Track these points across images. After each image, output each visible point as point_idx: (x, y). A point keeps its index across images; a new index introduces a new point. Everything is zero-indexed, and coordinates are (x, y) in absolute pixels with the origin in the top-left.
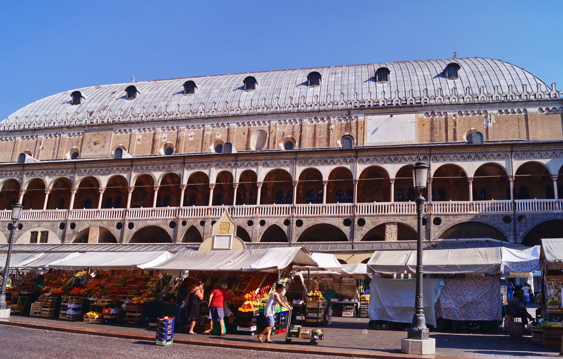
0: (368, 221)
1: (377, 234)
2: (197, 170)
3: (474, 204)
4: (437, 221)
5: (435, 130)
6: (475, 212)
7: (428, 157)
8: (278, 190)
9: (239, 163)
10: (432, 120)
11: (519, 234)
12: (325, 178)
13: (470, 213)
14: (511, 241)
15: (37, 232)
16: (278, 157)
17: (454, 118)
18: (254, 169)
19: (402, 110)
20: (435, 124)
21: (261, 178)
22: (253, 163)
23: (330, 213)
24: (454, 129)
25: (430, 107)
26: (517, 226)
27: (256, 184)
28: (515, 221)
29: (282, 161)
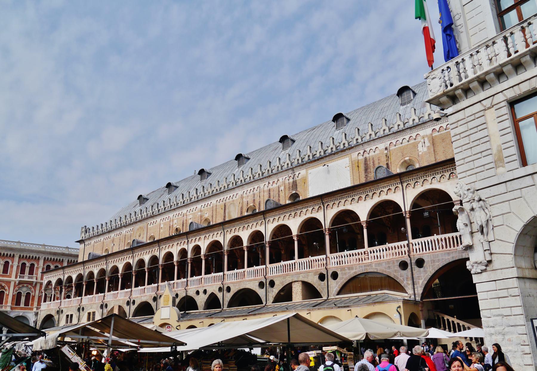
0: (277, 283)
1: (285, 295)
2: (167, 250)
4: (335, 276)
5: (369, 170)
6: (370, 261)
8: (216, 260)
9: (190, 240)
10: (366, 159)
11: (419, 282)
12: (245, 244)
13: (364, 262)
14: (410, 291)
17: (386, 152)
18: (199, 243)
19: (336, 156)
20: (368, 163)
21: (203, 252)
22: (198, 238)
23: (247, 278)
24: (387, 164)
25: (361, 146)
28: (411, 266)
29: (216, 233)
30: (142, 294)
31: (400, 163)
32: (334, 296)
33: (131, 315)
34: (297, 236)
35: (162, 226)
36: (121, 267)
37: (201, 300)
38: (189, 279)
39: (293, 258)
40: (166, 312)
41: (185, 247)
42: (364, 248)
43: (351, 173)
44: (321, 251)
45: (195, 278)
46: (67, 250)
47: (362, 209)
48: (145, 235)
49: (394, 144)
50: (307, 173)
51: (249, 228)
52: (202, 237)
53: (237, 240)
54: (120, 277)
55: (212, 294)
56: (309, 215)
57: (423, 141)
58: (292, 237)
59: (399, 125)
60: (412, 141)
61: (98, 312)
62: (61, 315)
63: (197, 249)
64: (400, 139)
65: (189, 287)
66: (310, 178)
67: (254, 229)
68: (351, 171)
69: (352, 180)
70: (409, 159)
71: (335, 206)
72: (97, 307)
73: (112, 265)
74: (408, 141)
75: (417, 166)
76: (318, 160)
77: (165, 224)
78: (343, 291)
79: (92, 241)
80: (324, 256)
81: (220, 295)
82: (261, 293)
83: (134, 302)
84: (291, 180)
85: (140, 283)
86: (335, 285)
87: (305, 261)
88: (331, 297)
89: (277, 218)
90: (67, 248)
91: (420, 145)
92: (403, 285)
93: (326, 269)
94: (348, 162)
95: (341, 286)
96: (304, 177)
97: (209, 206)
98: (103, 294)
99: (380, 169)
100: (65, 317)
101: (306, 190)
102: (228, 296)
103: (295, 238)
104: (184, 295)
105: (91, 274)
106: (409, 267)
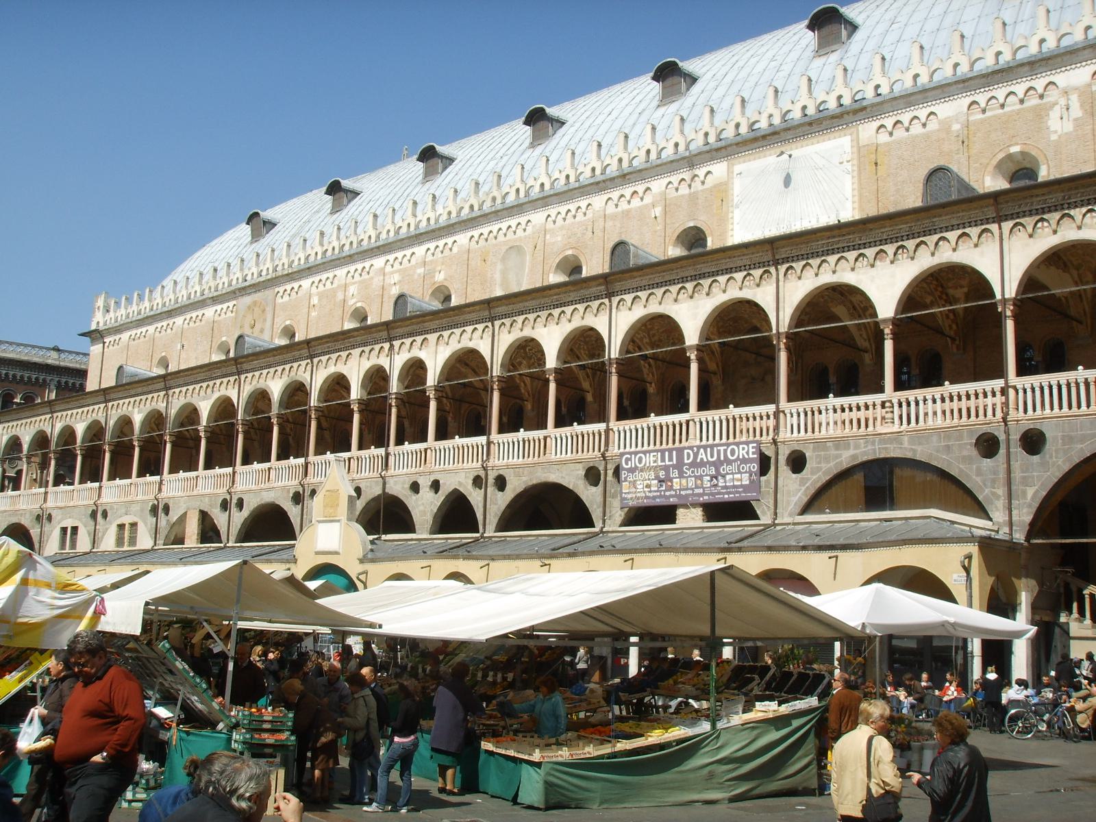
3: (895, 401)
4: (797, 462)
6: (896, 428)
7: (772, 270)
11: (1024, 493)
12: (551, 362)
14: (999, 515)
15: (124, 525)
16: (461, 318)
18: (422, 355)
21: (432, 379)
22: (419, 339)
26: (1016, 465)
27: (424, 391)
29: (469, 329)
30: (262, 482)
31: (994, 162)
32: (791, 515)
33: (232, 538)
34: (699, 348)
35: (315, 300)
36: (205, 409)
37: (424, 507)
38: (392, 448)
39: (685, 408)
40: (329, 535)
41: (384, 362)
42: (881, 390)
43: (856, 180)
44: (762, 391)
45: (407, 447)
46: (54, 354)
47: (884, 283)
48: (269, 323)
49: (983, 105)
50: (730, 171)
51: (564, 319)
52: (432, 337)
53: (527, 350)
54: (202, 434)
55: (456, 491)
56: (734, 293)
57: (1063, 102)
58: (684, 351)
59: (999, 54)
60: (1033, 101)
61: (146, 524)
62: (47, 528)
63: (416, 369)
64: (1000, 92)
65: (391, 472)
66: (737, 187)
67: (577, 323)
68: (855, 174)
69: (856, 199)
70: (1022, 153)
71: (809, 273)
72: (142, 510)
73: (182, 401)
74: (1022, 101)
75: (1044, 174)
76: (764, 137)
77: (321, 296)
78: (816, 504)
79: (125, 336)
80: (771, 408)
81: (475, 497)
82: (590, 495)
83: (240, 504)
84: (684, 190)
85: (257, 452)
86: (795, 488)
87: (717, 418)
88: (784, 518)
89: (643, 295)
90: (56, 349)
91: (1055, 114)
92: (980, 498)
93: (775, 442)
94: (848, 149)
95: (812, 491)
96: (721, 184)
97: (447, 252)
98: (157, 478)
99: (940, 174)
100: (56, 533)
101: (723, 221)
102: (500, 501)
103: (693, 356)
104: (377, 491)
105: (126, 422)
106: (1002, 451)
